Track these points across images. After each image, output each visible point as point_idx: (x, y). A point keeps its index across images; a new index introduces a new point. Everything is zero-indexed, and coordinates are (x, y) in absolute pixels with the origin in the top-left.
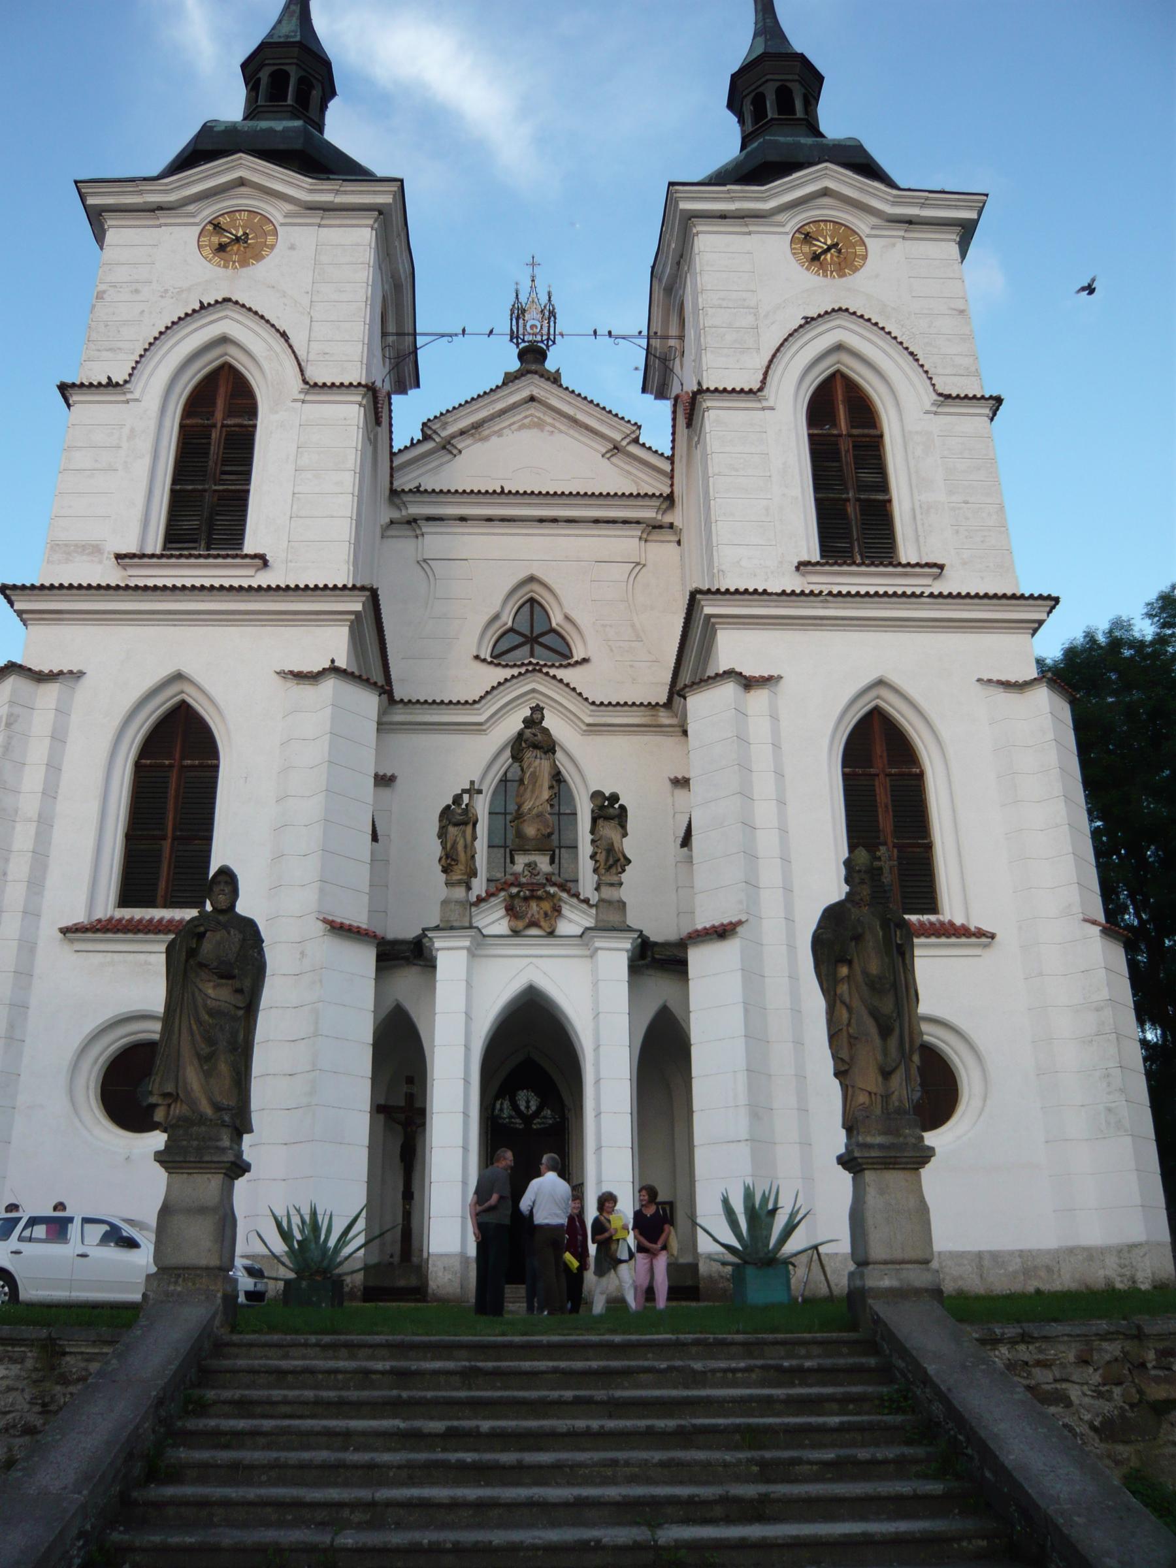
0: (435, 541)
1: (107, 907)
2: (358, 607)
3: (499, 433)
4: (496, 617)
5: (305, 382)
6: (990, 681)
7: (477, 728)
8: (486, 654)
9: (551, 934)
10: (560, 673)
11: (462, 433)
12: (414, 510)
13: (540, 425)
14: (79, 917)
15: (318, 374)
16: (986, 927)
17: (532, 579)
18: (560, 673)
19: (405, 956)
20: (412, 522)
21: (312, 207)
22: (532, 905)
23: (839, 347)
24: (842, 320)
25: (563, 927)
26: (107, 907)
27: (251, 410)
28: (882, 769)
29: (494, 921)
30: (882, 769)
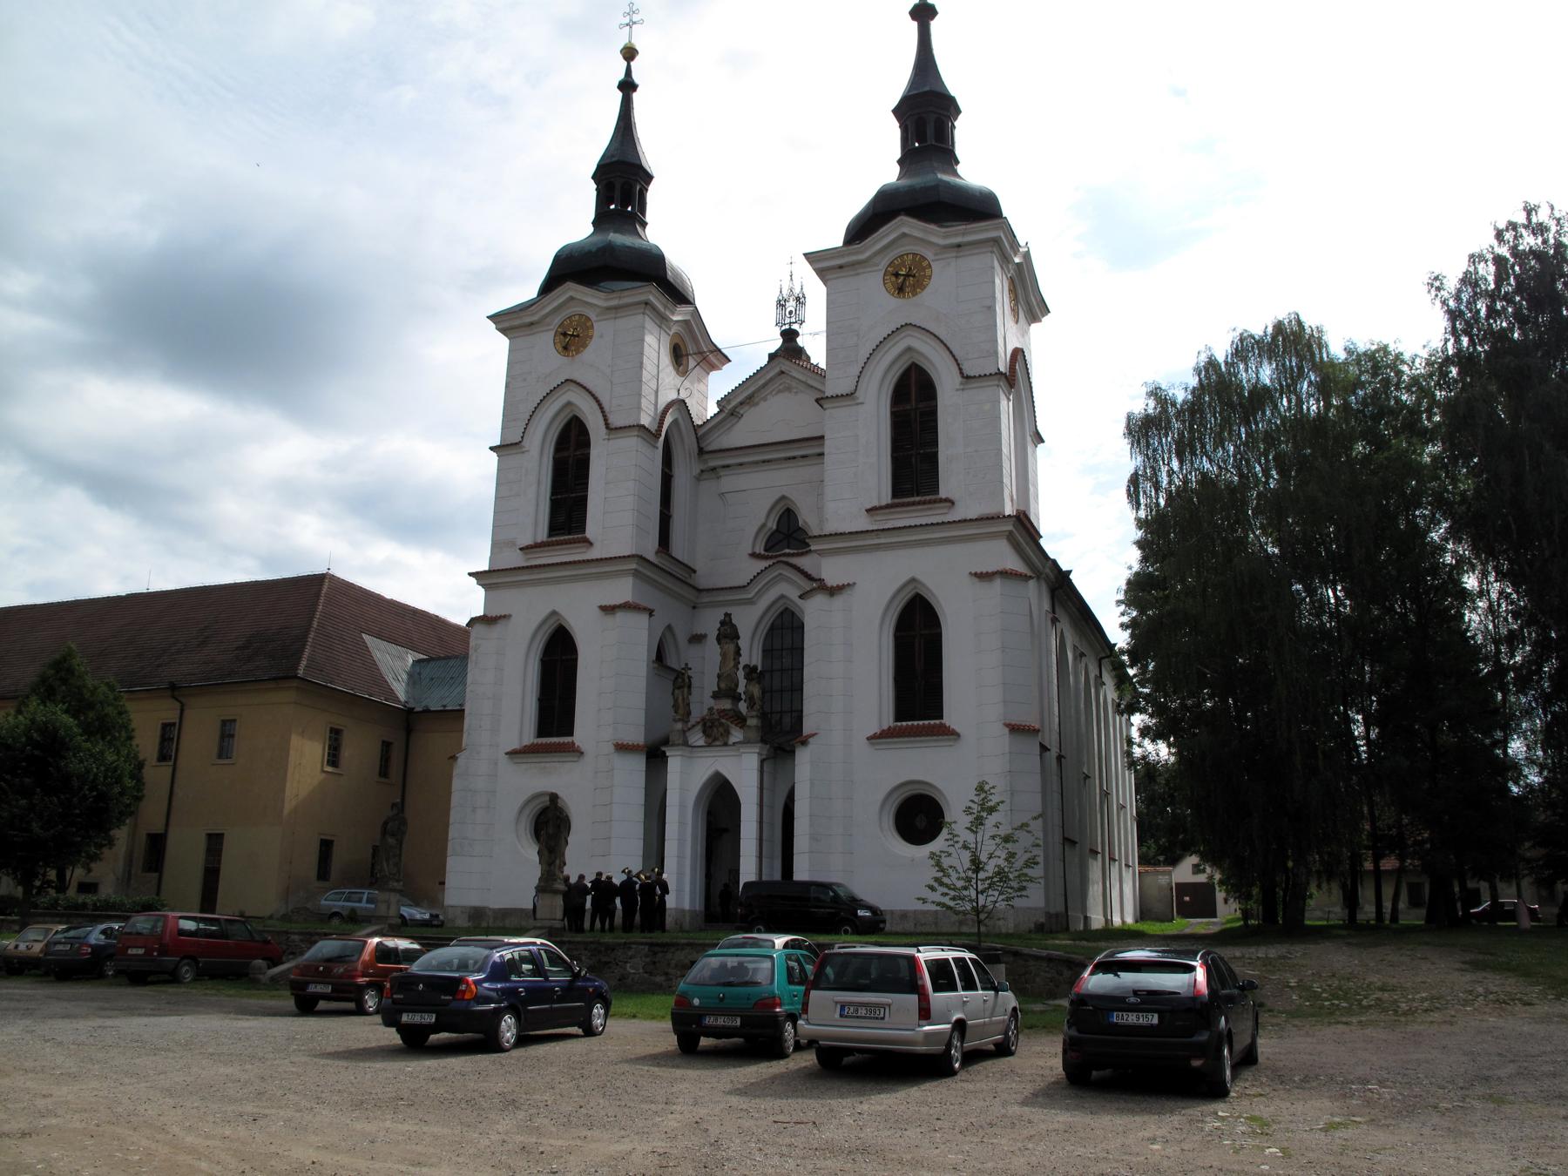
0: (729, 482)
1: (529, 737)
2: (634, 566)
3: (765, 399)
4: (764, 525)
5: (607, 425)
6: (976, 574)
7: (750, 602)
8: (760, 549)
9: (726, 744)
10: (794, 561)
11: (742, 403)
12: (712, 464)
13: (789, 389)
14: (516, 745)
15: (617, 421)
16: (958, 730)
17: (783, 498)
18: (794, 561)
19: (655, 756)
20: (714, 469)
21: (609, 309)
22: (715, 731)
23: (909, 349)
24: (910, 331)
25: (732, 740)
26: (529, 737)
27: (587, 444)
28: (917, 634)
29: (697, 738)
30: (917, 634)
